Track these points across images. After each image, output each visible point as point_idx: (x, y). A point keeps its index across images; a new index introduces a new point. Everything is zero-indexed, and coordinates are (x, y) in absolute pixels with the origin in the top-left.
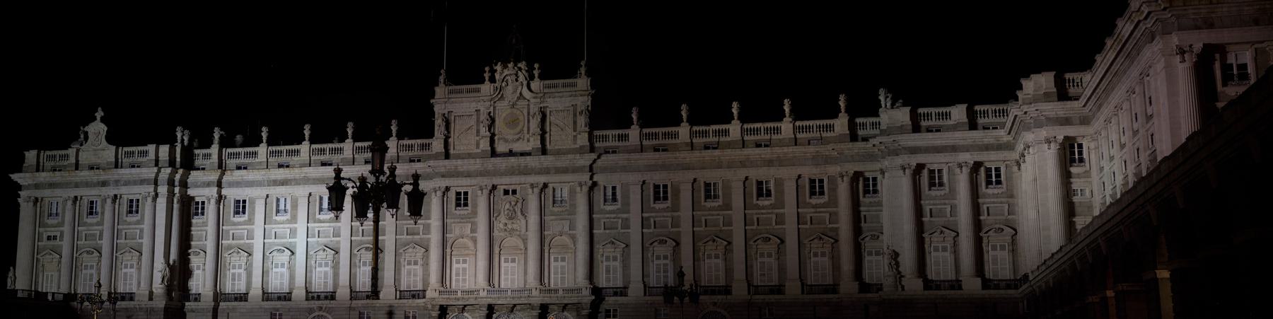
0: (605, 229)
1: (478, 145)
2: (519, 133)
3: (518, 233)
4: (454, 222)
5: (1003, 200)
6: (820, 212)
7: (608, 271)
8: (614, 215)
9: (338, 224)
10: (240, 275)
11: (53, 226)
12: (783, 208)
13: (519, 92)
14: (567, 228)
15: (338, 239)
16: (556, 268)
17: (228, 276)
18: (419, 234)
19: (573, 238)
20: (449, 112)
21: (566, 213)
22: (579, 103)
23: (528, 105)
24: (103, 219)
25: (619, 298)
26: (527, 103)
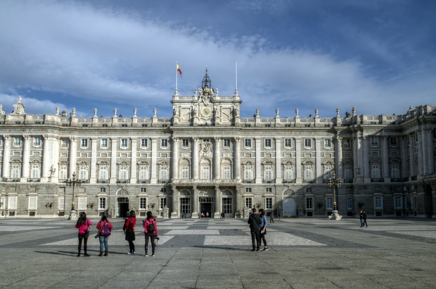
3: (209, 157)
4: (182, 152)
5: (397, 150)
6: (328, 152)
7: (247, 173)
10: (85, 172)
17: (79, 172)
20: (179, 106)
25: (251, 184)
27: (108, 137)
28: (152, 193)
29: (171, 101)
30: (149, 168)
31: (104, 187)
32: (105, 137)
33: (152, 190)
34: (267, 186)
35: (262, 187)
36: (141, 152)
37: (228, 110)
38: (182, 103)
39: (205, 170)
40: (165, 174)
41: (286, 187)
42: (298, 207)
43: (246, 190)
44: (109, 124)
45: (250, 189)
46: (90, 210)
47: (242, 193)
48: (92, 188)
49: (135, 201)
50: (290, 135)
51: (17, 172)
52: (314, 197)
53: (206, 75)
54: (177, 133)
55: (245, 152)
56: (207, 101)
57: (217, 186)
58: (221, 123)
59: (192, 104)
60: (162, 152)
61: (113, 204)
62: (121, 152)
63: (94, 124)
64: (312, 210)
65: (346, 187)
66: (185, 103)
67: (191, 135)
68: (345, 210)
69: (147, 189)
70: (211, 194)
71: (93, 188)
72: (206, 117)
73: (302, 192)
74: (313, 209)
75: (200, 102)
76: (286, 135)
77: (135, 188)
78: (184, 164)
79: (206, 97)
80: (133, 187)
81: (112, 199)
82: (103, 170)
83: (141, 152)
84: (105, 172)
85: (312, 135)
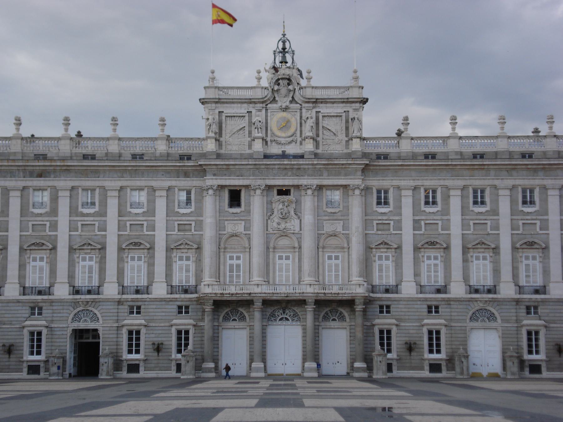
1: (250, 147)
2: (292, 136)
3: (292, 232)
4: (227, 220)
7: (381, 270)
8: (385, 218)
9: (103, 219)
12: (547, 214)
13: (291, 95)
14: (340, 229)
15: (103, 233)
19: (348, 238)
20: (219, 112)
21: (339, 214)
22: (351, 111)
23: (301, 109)
26: (298, 105)
27: (50, 183)
28: (155, 318)
29: (200, 100)
30: (150, 257)
31: (40, 305)
32: (42, 185)
33: (156, 310)
34: (431, 299)
35: (419, 303)
36: (130, 221)
37: (334, 119)
38: (227, 103)
39: (281, 261)
40: (188, 271)
41: (475, 304)
42: (506, 353)
43: (378, 310)
45: (388, 307)
46: (4, 360)
47: (370, 317)
48: (8, 308)
49: (115, 336)
50: (484, 179)
52: (546, 327)
53: (284, 35)
54: (214, 175)
55: (376, 220)
56: (285, 99)
57: (310, 301)
58: (319, 151)
59: (251, 105)
60: (180, 220)
61: (61, 344)
62: (81, 221)
63: (15, 153)
64: (541, 360)
66: (233, 103)
67: (247, 179)
69: (142, 307)
70: (296, 319)
71: (12, 308)
73: (516, 316)
74: (541, 356)
75: (269, 102)
76: (476, 179)
77: (116, 307)
78: (231, 248)
79: (283, 91)
80: (109, 303)
81: (58, 333)
82: (38, 263)
83: (130, 221)
84: (41, 269)
85: (539, 179)
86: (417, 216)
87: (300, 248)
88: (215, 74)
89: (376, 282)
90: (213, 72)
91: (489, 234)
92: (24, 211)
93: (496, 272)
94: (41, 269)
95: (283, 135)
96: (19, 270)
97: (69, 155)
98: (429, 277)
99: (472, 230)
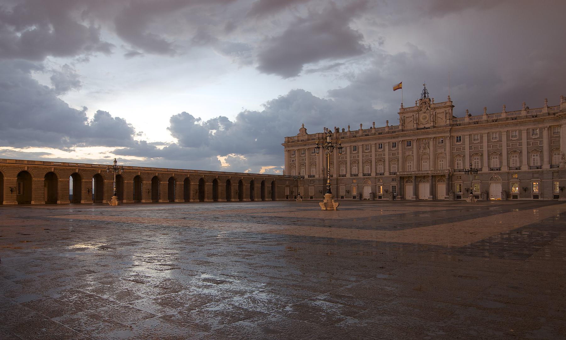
0: (457, 151)
1: (413, 126)
6: (536, 141)
7: (458, 164)
10: (344, 169)
11: (293, 157)
16: (440, 164)
18: (396, 155)
19: (446, 154)
22: (447, 110)
24: (305, 155)
25: (461, 173)
27: (357, 144)
37: (442, 114)
38: (406, 113)
44: (358, 135)
51: (304, 172)
52: (520, 182)
53: (425, 88)
54: (401, 137)
65: (553, 172)
68: (551, 194)
72: (424, 122)
84: (356, 169)
86: (471, 144)
87: (430, 158)
88: (403, 105)
89: (456, 168)
90: (402, 104)
91: (498, 149)
92: (351, 153)
93: (501, 163)
94: (356, 169)
95: (424, 121)
96: (350, 169)
97: (361, 135)
98: (475, 166)
99: (492, 148)
